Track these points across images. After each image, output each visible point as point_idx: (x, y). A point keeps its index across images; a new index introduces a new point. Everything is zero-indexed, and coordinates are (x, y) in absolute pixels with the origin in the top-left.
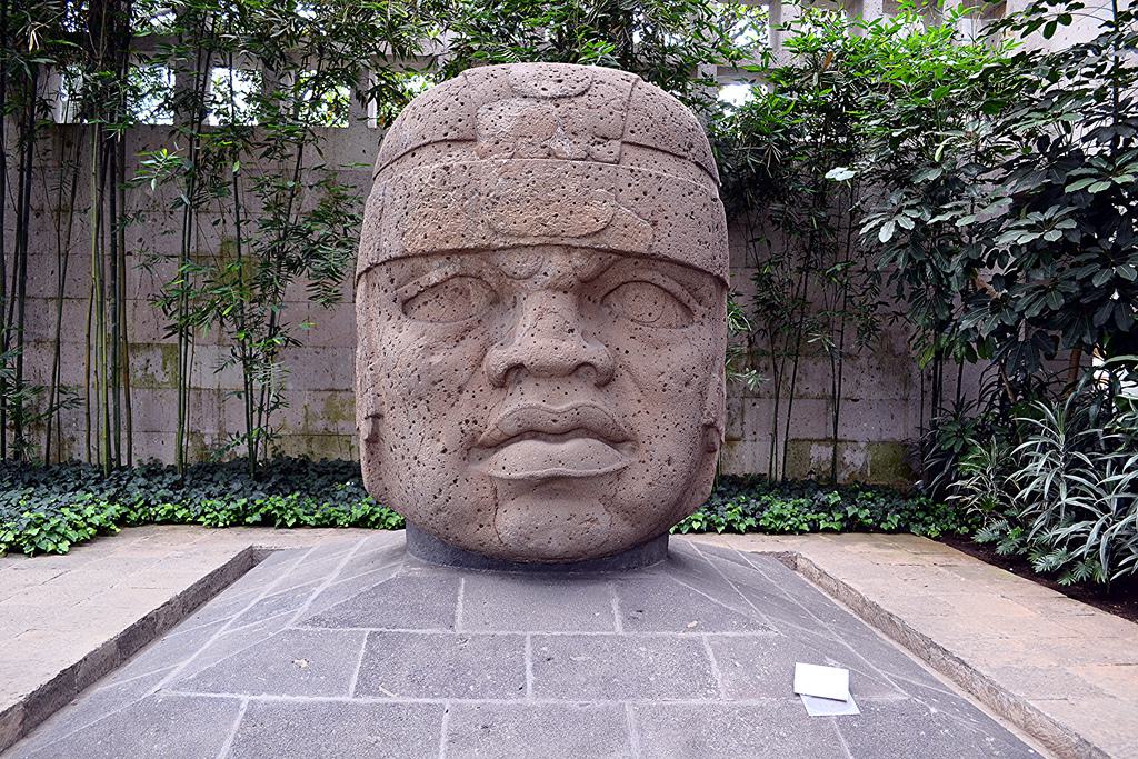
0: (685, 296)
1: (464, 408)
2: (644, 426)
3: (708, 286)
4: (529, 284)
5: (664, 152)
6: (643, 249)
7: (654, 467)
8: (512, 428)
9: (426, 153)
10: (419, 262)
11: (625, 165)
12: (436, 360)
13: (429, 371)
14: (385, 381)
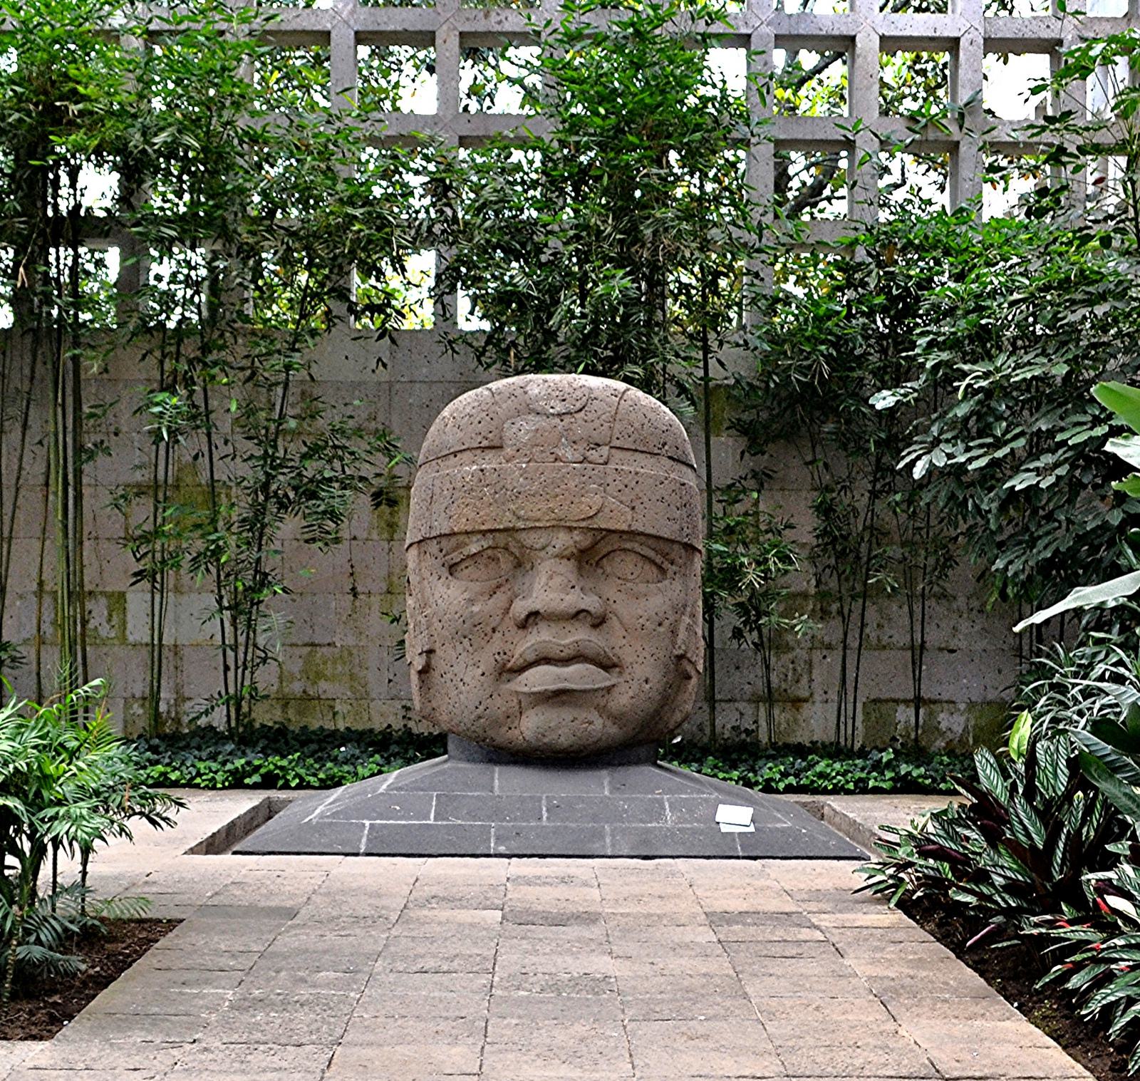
0: (659, 559)
1: (497, 643)
2: (627, 655)
3: (677, 552)
4: (543, 554)
5: (642, 452)
6: (624, 527)
7: (635, 685)
8: (531, 657)
9: (466, 456)
10: (461, 538)
11: (612, 466)
12: (476, 609)
13: (471, 617)
14: (437, 625)
